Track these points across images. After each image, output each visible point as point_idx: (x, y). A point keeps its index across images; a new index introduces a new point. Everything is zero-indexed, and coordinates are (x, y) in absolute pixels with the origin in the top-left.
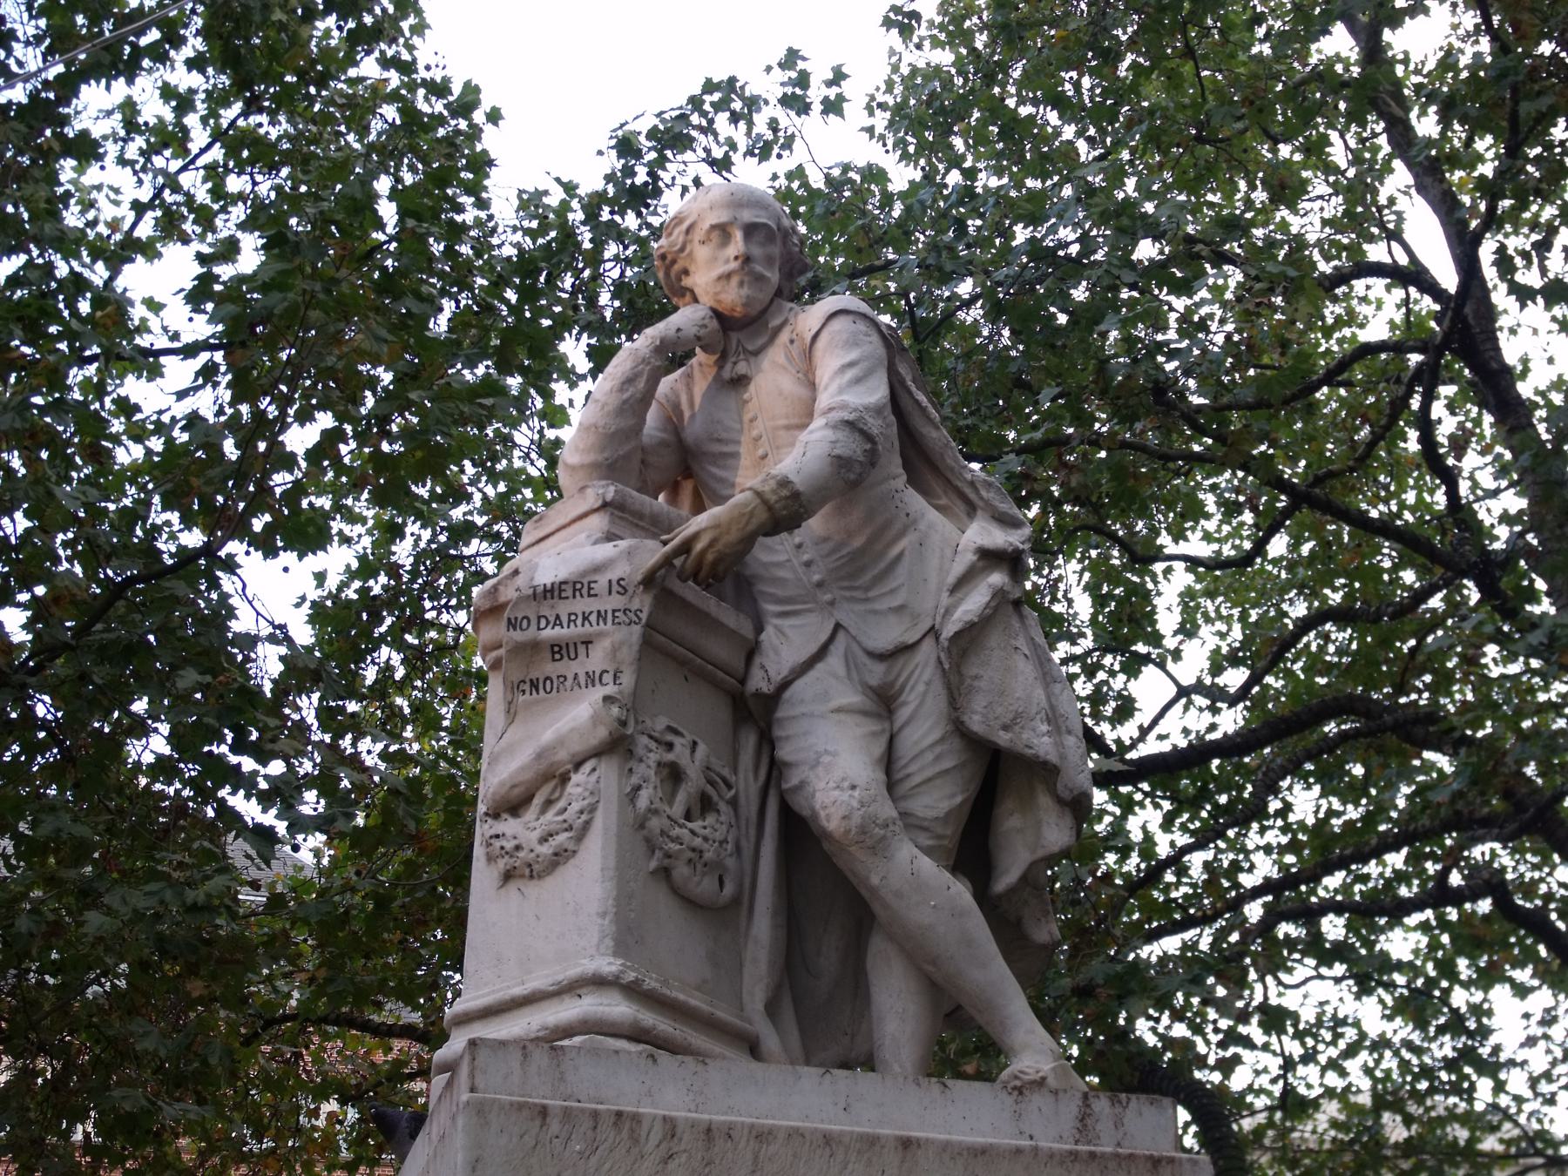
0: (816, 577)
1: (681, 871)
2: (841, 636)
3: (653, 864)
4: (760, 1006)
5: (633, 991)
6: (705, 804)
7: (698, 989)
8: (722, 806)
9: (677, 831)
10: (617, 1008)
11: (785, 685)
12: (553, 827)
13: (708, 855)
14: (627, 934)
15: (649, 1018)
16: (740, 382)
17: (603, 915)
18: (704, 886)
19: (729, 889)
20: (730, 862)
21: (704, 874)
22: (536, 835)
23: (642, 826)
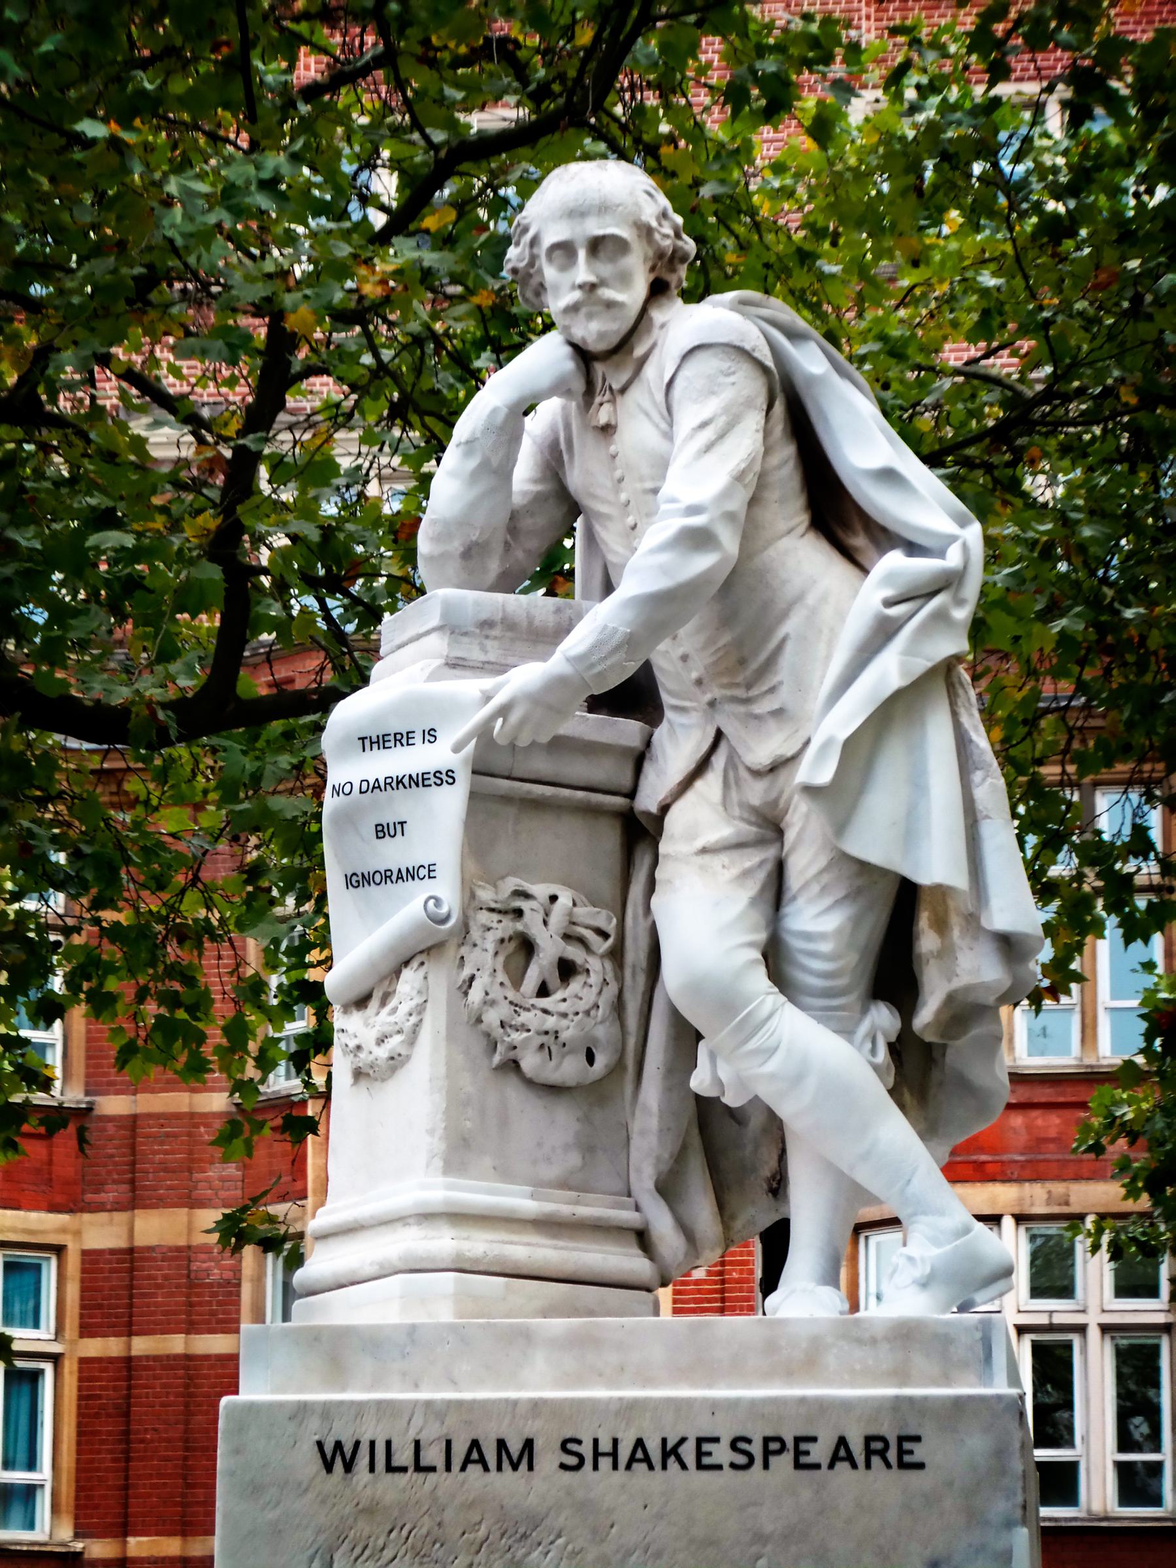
0: (694, 675)
1: (530, 1062)
3: (497, 1059)
4: (650, 1184)
5: (459, 1217)
6: (567, 970)
7: (564, 1184)
8: (594, 964)
9: (525, 1017)
10: (444, 1242)
11: (665, 809)
12: (387, 1029)
13: (564, 1036)
15: (480, 1244)
16: (607, 430)
17: (431, 1132)
19: (602, 1060)
21: (563, 1056)
22: (373, 1034)
23: (479, 1020)
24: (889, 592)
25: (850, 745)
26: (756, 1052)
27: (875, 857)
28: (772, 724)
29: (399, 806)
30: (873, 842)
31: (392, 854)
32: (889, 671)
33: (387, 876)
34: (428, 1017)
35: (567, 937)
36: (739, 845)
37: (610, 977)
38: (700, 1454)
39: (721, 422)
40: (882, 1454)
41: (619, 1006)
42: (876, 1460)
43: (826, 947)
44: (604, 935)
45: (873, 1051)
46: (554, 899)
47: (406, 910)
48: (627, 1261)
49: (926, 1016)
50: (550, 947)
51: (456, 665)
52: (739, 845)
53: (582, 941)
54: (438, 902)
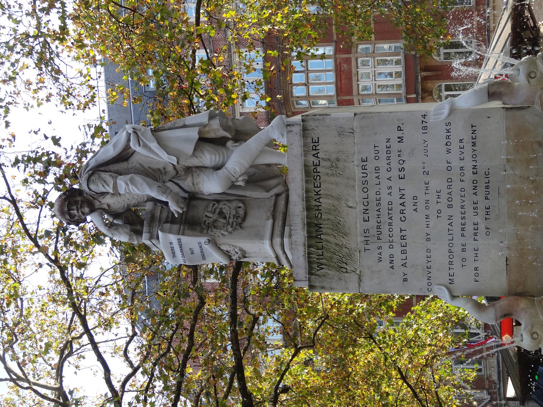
2: (173, 180)
4: (267, 193)
8: (220, 206)
9: (231, 222)
14: (259, 236)
15: (277, 231)
17: (255, 243)
18: (241, 212)
20: (234, 205)
23: (231, 232)
24: (137, 146)
25: (168, 154)
26: (235, 173)
27: (193, 147)
28: (166, 170)
29: (186, 249)
30: (189, 148)
31: (197, 251)
32: (154, 145)
33: (202, 252)
34: (230, 243)
35: (214, 213)
36: (192, 176)
37: (223, 203)
38: (317, 187)
39: (103, 182)
40: (316, 147)
41: (229, 201)
42: (317, 148)
43: (213, 157)
44: (214, 204)
45: (237, 146)
46: (206, 216)
47: (208, 249)
48: (282, 198)
49: (228, 135)
50: (215, 216)
51: (158, 238)
52: (192, 176)
53: (215, 209)
54: (205, 242)
